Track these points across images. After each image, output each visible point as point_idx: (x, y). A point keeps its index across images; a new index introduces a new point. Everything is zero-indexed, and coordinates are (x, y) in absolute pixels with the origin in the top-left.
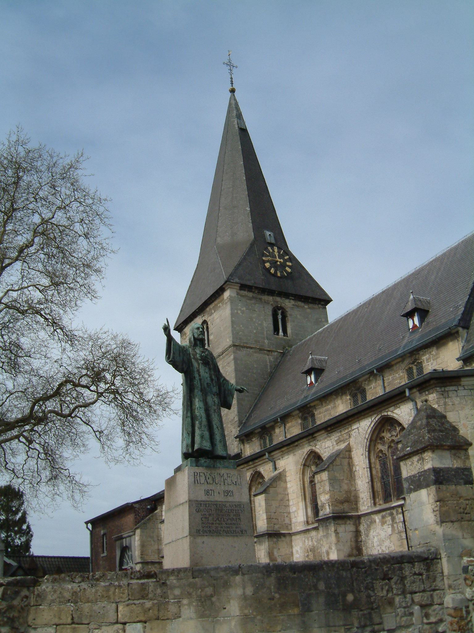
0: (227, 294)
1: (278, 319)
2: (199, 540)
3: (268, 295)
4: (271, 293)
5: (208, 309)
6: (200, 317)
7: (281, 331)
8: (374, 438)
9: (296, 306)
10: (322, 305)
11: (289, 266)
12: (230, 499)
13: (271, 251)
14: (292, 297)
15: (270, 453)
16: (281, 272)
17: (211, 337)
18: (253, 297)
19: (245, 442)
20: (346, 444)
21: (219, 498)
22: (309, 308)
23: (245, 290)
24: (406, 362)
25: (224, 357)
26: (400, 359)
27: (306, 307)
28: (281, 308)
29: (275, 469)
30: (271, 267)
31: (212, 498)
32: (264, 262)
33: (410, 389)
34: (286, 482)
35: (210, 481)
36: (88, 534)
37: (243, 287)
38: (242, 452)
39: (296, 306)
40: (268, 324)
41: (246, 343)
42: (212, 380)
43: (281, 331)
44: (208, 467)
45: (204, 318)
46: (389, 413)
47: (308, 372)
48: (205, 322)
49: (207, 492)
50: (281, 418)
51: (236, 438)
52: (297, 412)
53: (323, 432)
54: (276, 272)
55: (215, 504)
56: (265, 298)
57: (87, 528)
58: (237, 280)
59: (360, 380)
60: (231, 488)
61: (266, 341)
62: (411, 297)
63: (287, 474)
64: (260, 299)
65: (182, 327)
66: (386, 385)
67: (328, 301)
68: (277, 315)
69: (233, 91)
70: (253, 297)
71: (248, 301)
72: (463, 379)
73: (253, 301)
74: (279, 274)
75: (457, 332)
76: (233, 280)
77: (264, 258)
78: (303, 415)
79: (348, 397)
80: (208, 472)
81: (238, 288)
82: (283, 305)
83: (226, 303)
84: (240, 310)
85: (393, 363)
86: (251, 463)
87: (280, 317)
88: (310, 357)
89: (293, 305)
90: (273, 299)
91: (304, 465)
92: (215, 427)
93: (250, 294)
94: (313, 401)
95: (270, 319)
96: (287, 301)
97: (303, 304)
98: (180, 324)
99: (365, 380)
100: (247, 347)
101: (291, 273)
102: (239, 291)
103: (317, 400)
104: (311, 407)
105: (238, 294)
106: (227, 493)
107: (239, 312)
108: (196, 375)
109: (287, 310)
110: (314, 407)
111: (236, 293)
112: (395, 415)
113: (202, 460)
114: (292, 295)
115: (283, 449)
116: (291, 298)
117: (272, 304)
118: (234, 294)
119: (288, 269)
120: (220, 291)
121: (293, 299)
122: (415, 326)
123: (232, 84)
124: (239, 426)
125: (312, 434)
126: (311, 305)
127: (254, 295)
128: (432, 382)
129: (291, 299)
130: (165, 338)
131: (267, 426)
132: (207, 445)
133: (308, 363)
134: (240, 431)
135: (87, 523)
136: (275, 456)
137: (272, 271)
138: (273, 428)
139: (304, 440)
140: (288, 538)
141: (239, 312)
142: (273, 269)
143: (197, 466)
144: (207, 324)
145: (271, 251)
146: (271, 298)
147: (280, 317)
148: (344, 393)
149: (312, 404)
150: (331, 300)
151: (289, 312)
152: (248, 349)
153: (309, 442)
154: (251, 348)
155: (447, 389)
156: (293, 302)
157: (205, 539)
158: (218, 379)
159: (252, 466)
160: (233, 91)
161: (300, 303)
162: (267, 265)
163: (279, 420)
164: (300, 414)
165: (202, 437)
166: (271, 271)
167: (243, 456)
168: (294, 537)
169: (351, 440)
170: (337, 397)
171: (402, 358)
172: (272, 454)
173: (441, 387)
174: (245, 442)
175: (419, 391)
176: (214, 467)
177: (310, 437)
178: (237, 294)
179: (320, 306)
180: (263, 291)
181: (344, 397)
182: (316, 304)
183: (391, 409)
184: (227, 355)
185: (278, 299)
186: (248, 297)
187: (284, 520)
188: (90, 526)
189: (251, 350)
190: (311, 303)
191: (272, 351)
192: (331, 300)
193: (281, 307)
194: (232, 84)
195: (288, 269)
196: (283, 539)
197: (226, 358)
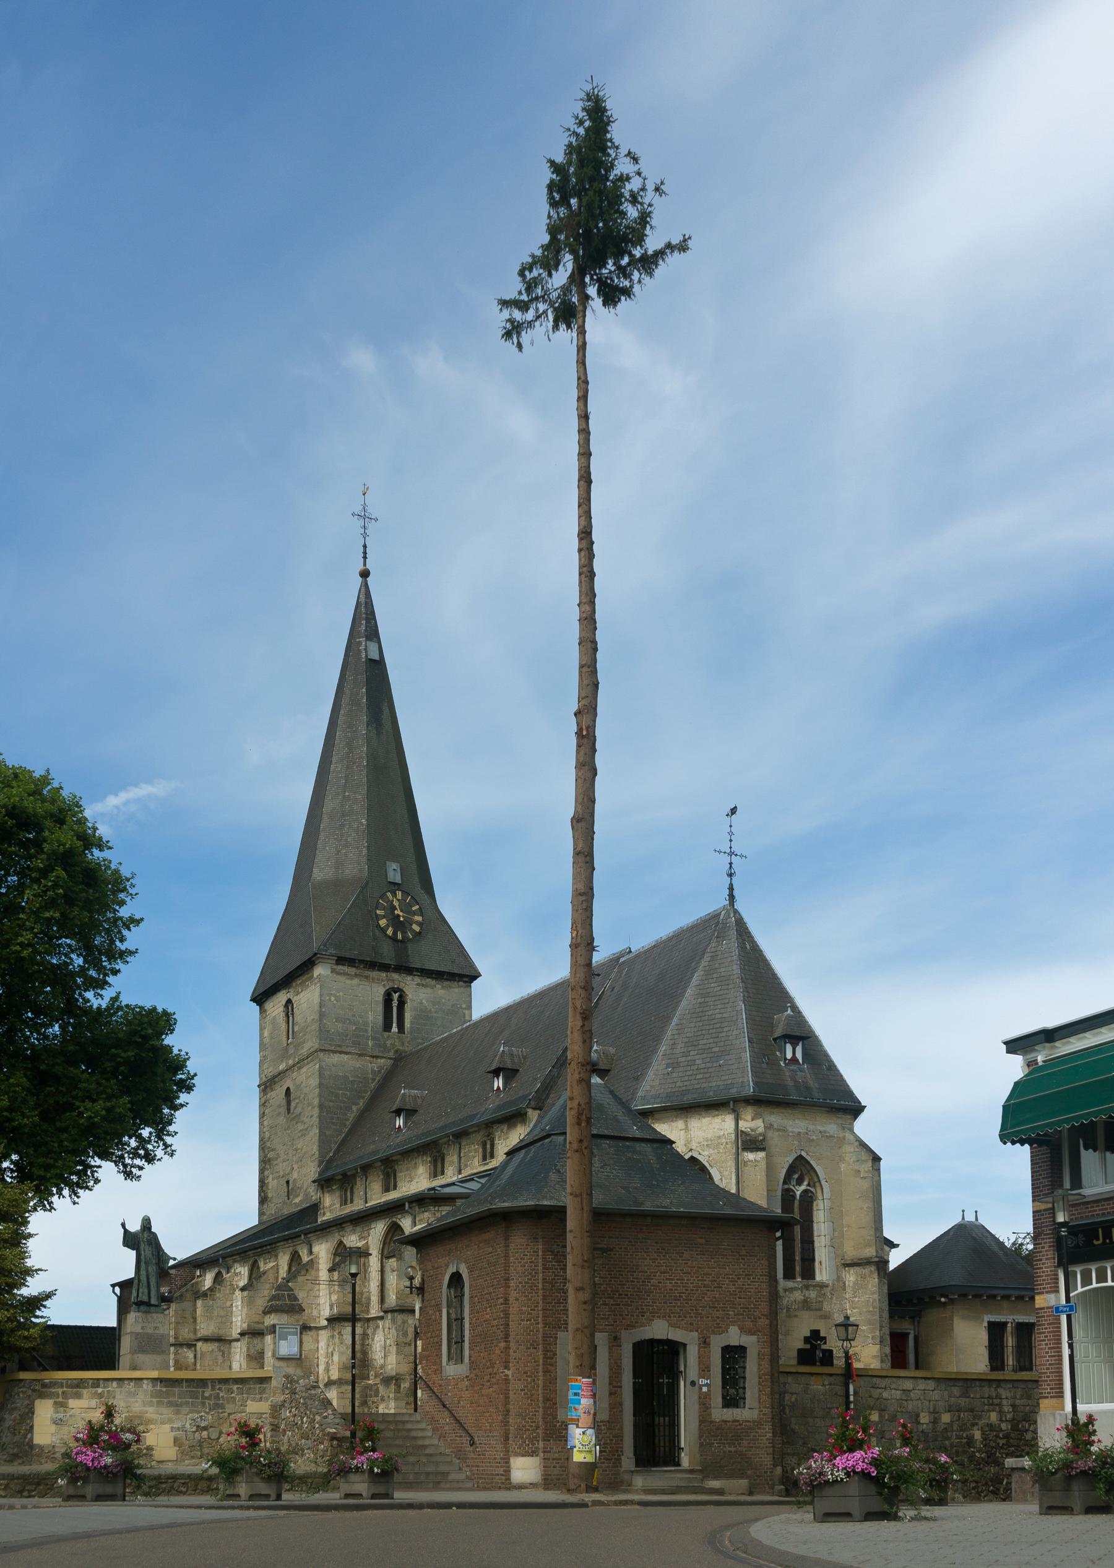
0: (319, 971)
2: (136, 1356)
3: (379, 970)
4: (385, 968)
5: (294, 984)
6: (284, 991)
7: (395, 1025)
8: (388, 1241)
9: (423, 985)
10: (465, 982)
11: (417, 923)
12: (157, 1332)
14: (418, 972)
15: (306, 1234)
16: (404, 933)
17: (296, 1029)
18: (356, 975)
19: (325, 1190)
20: (364, 1242)
21: (150, 1331)
22: (443, 988)
24: (481, 1133)
25: (308, 1063)
26: (476, 1129)
28: (395, 990)
29: (311, 1252)
30: (388, 926)
31: (145, 1331)
32: (378, 918)
33: (410, 1203)
34: (318, 1270)
35: (145, 1321)
36: (114, 1300)
37: (341, 960)
38: (320, 1202)
40: (375, 1016)
41: (340, 1046)
42: (153, 1255)
43: (395, 1025)
44: (145, 1312)
45: (289, 996)
46: (398, 1220)
47: (398, 1112)
48: (289, 1001)
49: (143, 1328)
50: (361, 1168)
51: (314, 1182)
52: (380, 1164)
53: (349, 1224)
54: (395, 933)
55: (148, 1334)
56: (375, 974)
57: (114, 1292)
58: (332, 951)
59: (440, 1141)
60: (158, 1325)
61: (370, 1043)
62: (502, 1049)
63: (321, 1261)
64: (367, 977)
65: (261, 999)
66: (462, 1155)
68: (392, 1000)
71: (349, 982)
72: (457, 1200)
73: (356, 981)
74: (400, 936)
75: (526, 1114)
76: (326, 951)
77: (378, 912)
78: (385, 1169)
79: (429, 1159)
80: (144, 1315)
81: (334, 962)
83: (316, 984)
84: (335, 996)
85: (470, 1130)
86: (290, 1241)
87: (395, 1004)
88: (403, 1091)
89: (418, 984)
90: (387, 976)
91: (335, 1254)
92: (152, 1286)
93: (352, 971)
94: (392, 1155)
95: (380, 1008)
96: (409, 978)
97: (433, 982)
98: (259, 995)
99: (445, 1143)
100: (341, 1052)
101: (420, 933)
102: (335, 967)
103: (399, 1154)
104: (393, 1161)
106: (156, 1328)
107: (333, 999)
108: (143, 1253)
109: (407, 993)
110: (396, 1161)
111: (330, 970)
112: (401, 1224)
113: (142, 1308)
114: (417, 970)
115: (317, 1233)
116: (415, 973)
119: (416, 928)
120: (307, 966)
121: (418, 976)
122: (498, 1088)
124: (319, 1166)
125: (341, 1224)
127: (358, 972)
128: (426, 1201)
129: (415, 975)
130: (122, 1231)
131: (349, 1173)
132: (145, 1299)
133: (397, 1102)
134: (320, 1174)
135: (113, 1286)
136: (312, 1239)
137: (390, 932)
138: (354, 1176)
139: (334, 1228)
140: (313, 1333)
141: (333, 999)
142: (390, 929)
143: (138, 1311)
144: (293, 1005)
147: (395, 1004)
148: (425, 1153)
149: (395, 1158)
150: (481, 975)
151: (410, 994)
152: (342, 1055)
153: (339, 1231)
155: (440, 1209)
156: (417, 980)
157: (140, 1355)
158: (158, 1253)
159: (292, 1244)
161: (429, 981)
162: (383, 922)
163: (359, 1170)
164: (382, 1168)
165: (143, 1293)
166: (388, 932)
167: (321, 1207)
168: (320, 1332)
169: (370, 1238)
170: (419, 1156)
171: (479, 1127)
172: (309, 1236)
173: (435, 1206)
174: (325, 1190)
175: (419, 1205)
176: (149, 1312)
177: (339, 1226)
178: (332, 972)
179: (461, 983)
180: (373, 965)
181: (425, 1158)
182: (455, 980)
183: (399, 1216)
184: (311, 1061)
185: (395, 976)
186: (349, 975)
187: (312, 1313)
188: (117, 1290)
189: (347, 1056)
190: (447, 980)
191: (377, 1057)
192: (481, 975)
193: (398, 988)
195: (416, 928)
196: (309, 1333)
197: (311, 1065)
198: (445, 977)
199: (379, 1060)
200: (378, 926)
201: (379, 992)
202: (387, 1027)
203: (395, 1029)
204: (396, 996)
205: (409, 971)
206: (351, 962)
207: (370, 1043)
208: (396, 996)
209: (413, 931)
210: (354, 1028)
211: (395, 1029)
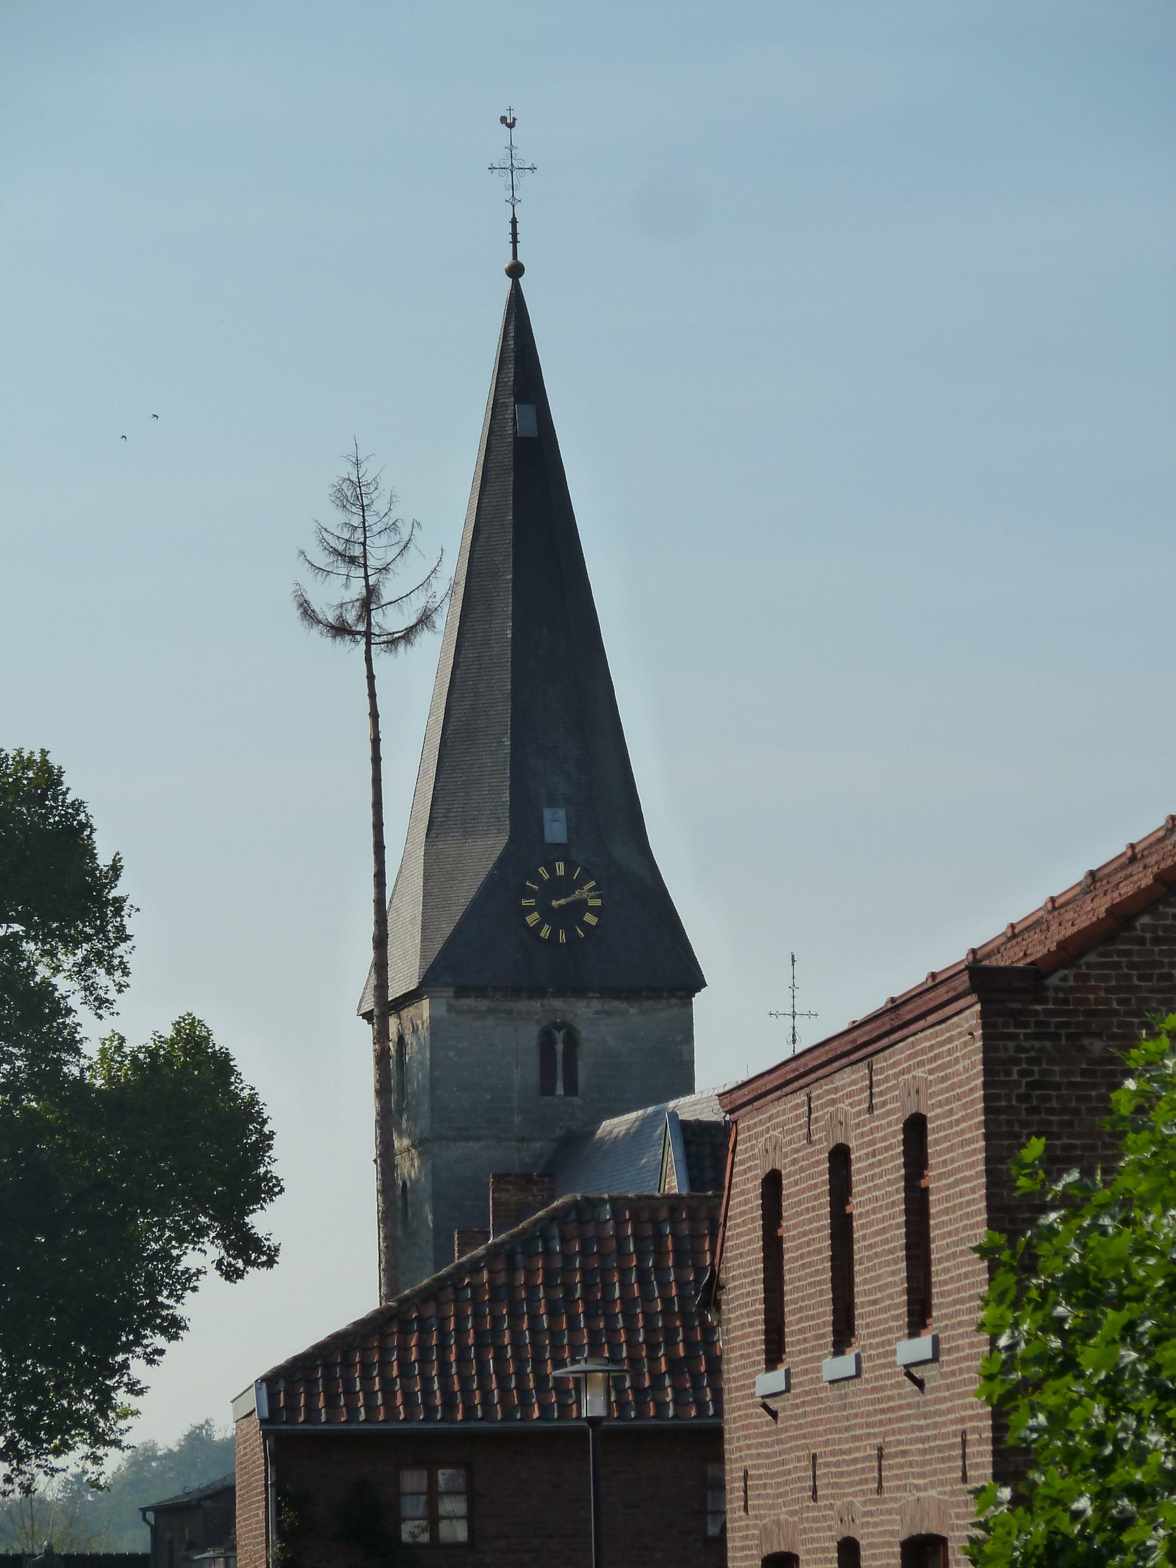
1: (556, 1054)
3: (530, 997)
4: (537, 992)
9: (606, 1012)
10: (681, 998)
13: (546, 876)
18: (490, 1011)
23: (468, 997)
27: (634, 1011)
37: (461, 991)
39: (606, 1012)
54: (554, 933)
56: (522, 1005)
57: (144, 1519)
64: (509, 1012)
67: (703, 984)
68: (554, 1043)
69: (516, 271)
70: (490, 1011)
74: (562, 938)
77: (524, 902)
81: (451, 994)
82: (569, 1016)
87: (560, 1048)
89: (598, 1012)
90: (542, 1006)
93: (484, 1004)
95: (533, 1060)
96: (582, 1004)
97: (625, 1005)
102: (454, 1002)
105: (451, 1008)
107: (451, 1054)
116: (591, 995)
117: (538, 1021)
118: (442, 1011)
119: (590, 919)
121: (597, 998)
123: (515, 242)
126: (647, 1004)
135: (144, 1511)
142: (546, 927)
145: (546, 876)
146: (536, 1005)
147: (560, 1048)
152: (471, 1144)
154: (478, 1139)
156: (596, 1005)
160: (516, 271)
161: (616, 1004)
162: (532, 919)
178: (449, 1011)
179: (673, 1001)
185: (558, 1003)
188: (150, 1516)
194: (515, 242)
198: (644, 994)
199: (532, 1145)
200: (526, 925)
201: (530, 1034)
202: (547, 1087)
203: (560, 1090)
204: (559, 1036)
205: (579, 991)
206: (480, 992)
207: (517, 1119)
208: (559, 1036)
209: (585, 926)
210: (488, 1097)
211: (560, 1090)
